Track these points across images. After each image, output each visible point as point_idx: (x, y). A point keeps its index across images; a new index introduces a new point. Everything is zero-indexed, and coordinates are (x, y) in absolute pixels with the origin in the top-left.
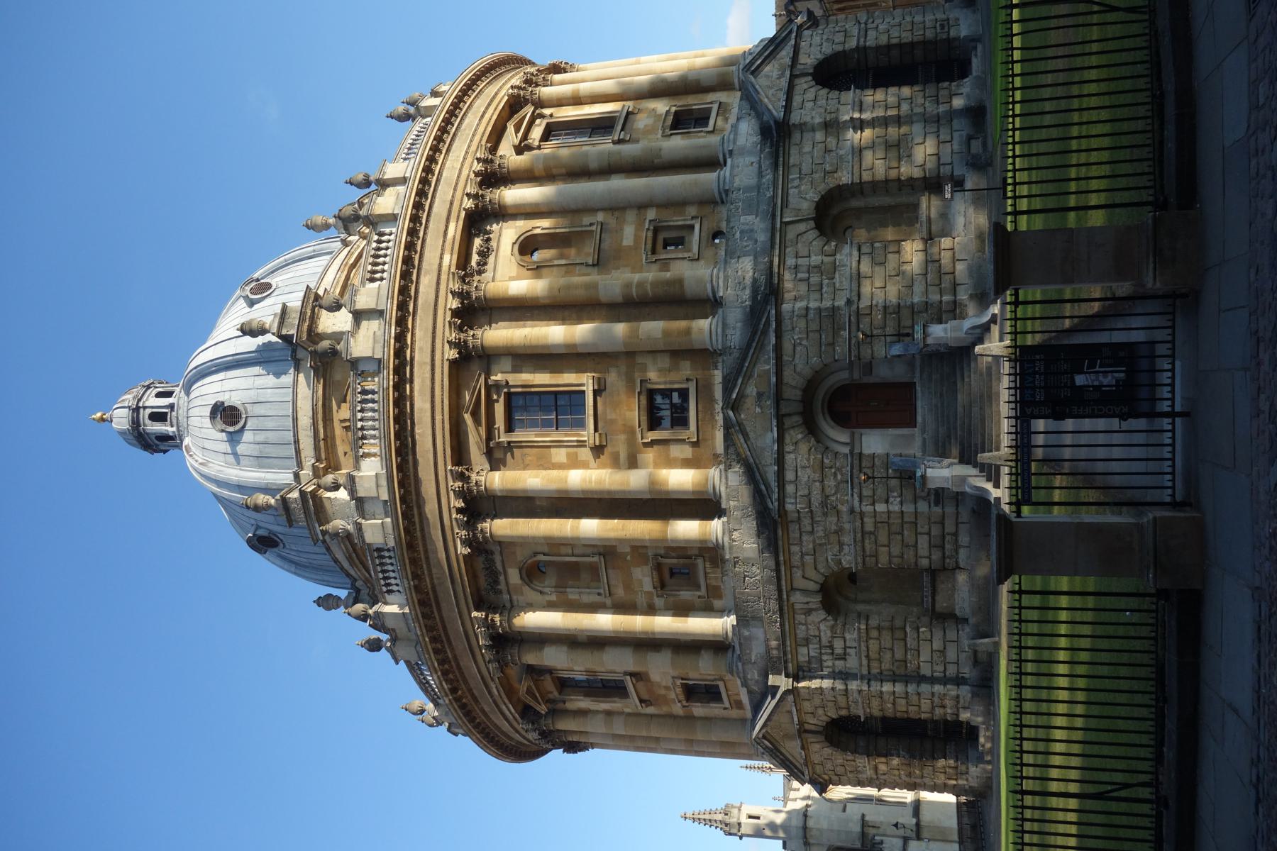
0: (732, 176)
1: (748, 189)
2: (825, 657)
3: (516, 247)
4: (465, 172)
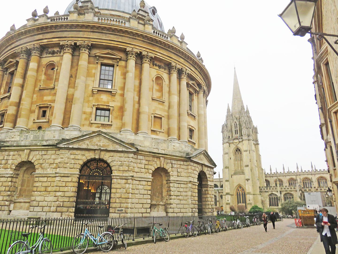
1: (43, 136)
4: (79, 39)
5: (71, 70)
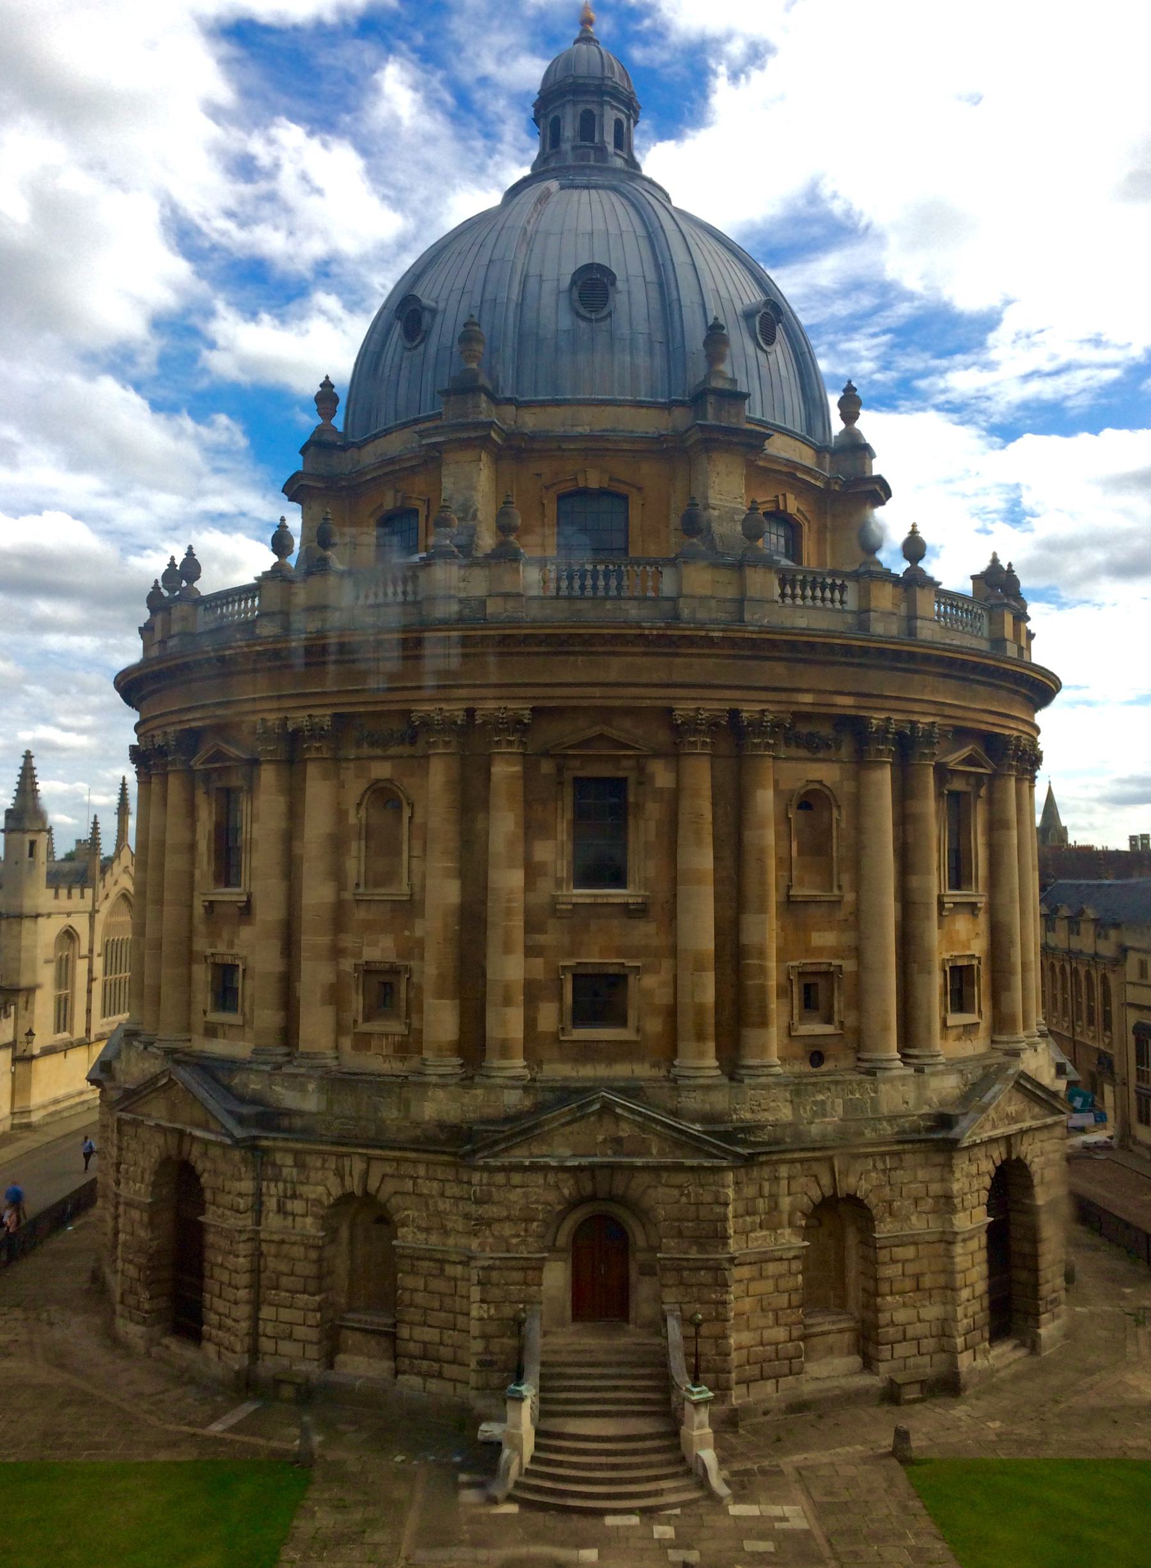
0: (890, 1081)
2: (281, 1185)
3: (817, 786)
4: (917, 707)
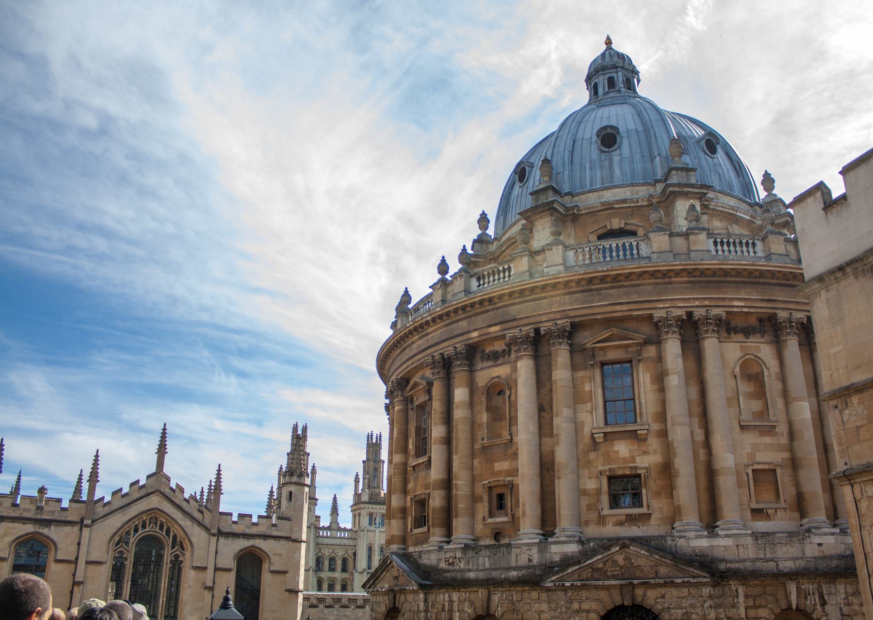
5: (538, 392)
